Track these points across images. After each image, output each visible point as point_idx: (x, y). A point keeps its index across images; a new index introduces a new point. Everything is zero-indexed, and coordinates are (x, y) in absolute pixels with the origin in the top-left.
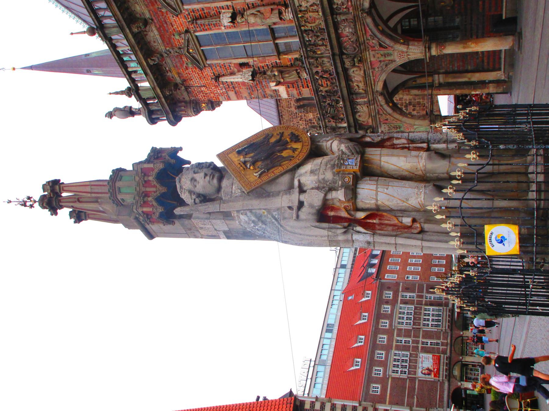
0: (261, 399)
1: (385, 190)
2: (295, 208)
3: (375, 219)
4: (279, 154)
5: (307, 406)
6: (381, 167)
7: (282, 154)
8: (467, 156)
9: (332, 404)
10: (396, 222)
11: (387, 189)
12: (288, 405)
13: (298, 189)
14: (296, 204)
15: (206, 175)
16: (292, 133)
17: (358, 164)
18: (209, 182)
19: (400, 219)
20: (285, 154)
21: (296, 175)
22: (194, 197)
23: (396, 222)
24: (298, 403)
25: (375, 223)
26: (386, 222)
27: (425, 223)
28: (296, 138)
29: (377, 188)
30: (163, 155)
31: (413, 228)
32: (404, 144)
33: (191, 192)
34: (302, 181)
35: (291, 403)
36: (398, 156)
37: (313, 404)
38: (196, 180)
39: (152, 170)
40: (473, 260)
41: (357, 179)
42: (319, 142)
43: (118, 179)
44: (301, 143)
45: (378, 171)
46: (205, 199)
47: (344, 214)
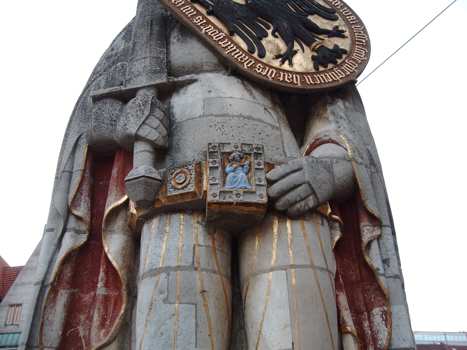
1: (162, 296)
3: (106, 285)
4: (270, 32)
6: (255, 275)
7: (270, 37)
11: (166, 301)
13: (163, 79)
16: (344, 52)
17: (228, 200)
20: (273, 43)
25: (97, 287)
26: (96, 318)
29: (167, 270)
32: (375, 340)
34: (191, 88)
41: (192, 205)
42: (333, 113)
44: (313, 71)
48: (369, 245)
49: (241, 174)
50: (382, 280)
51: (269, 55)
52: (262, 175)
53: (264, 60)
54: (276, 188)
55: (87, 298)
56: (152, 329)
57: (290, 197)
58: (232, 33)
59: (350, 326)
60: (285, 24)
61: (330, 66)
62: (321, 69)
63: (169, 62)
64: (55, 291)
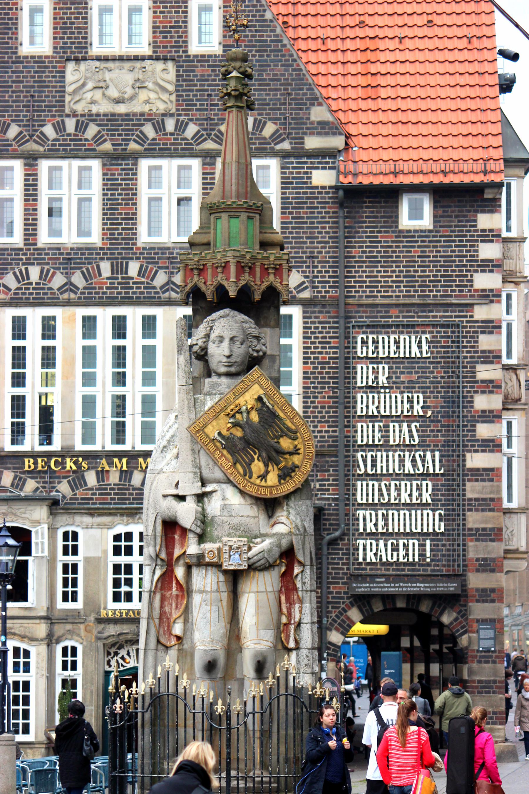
0: (504, 67)
2: (175, 492)
3: (177, 589)
4: (256, 457)
5: (485, 221)
7: (256, 461)
8: (220, 702)
9: (500, 291)
10: (174, 616)
12: (480, 166)
13: (199, 492)
14: (181, 493)
15: (228, 357)
16: (297, 467)
18: (220, 362)
19: (181, 620)
21: (224, 486)
22: (200, 343)
23: (174, 616)
24: (488, 194)
27: (179, 650)
28: (285, 475)
30: (272, 278)
31: (169, 637)
33: (208, 336)
34: (214, 494)
35: (485, 173)
36: (257, 613)
37: (490, 236)
38: (221, 342)
39: (228, 279)
40: (118, 709)
42: (287, 505)
43: (232, 214)
45: (239, 589)
46: (202, 356)
47: (177, 552)
48: (297, 575)
49: (237, 556)
50: (300, 593)
51: (255, 476)
52: (245, 556)
53: (252, 480)
54: (252, 561)
55: (168, 594)
56: (201, 615)
57: (258, 564)
58: (235, 464)
59: (285, 610)
60: (264, 454)
61: (288, 479)
62: (282, 481)
63: (201, 472)
64: (155, 593)
